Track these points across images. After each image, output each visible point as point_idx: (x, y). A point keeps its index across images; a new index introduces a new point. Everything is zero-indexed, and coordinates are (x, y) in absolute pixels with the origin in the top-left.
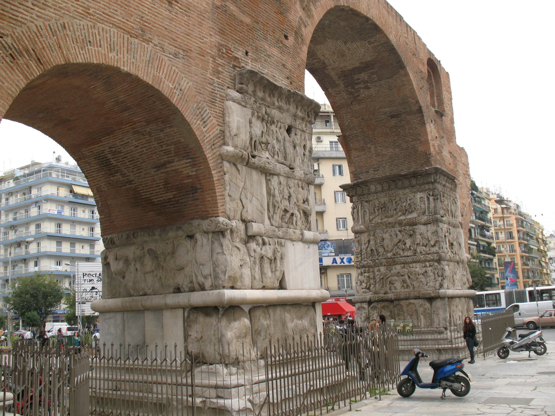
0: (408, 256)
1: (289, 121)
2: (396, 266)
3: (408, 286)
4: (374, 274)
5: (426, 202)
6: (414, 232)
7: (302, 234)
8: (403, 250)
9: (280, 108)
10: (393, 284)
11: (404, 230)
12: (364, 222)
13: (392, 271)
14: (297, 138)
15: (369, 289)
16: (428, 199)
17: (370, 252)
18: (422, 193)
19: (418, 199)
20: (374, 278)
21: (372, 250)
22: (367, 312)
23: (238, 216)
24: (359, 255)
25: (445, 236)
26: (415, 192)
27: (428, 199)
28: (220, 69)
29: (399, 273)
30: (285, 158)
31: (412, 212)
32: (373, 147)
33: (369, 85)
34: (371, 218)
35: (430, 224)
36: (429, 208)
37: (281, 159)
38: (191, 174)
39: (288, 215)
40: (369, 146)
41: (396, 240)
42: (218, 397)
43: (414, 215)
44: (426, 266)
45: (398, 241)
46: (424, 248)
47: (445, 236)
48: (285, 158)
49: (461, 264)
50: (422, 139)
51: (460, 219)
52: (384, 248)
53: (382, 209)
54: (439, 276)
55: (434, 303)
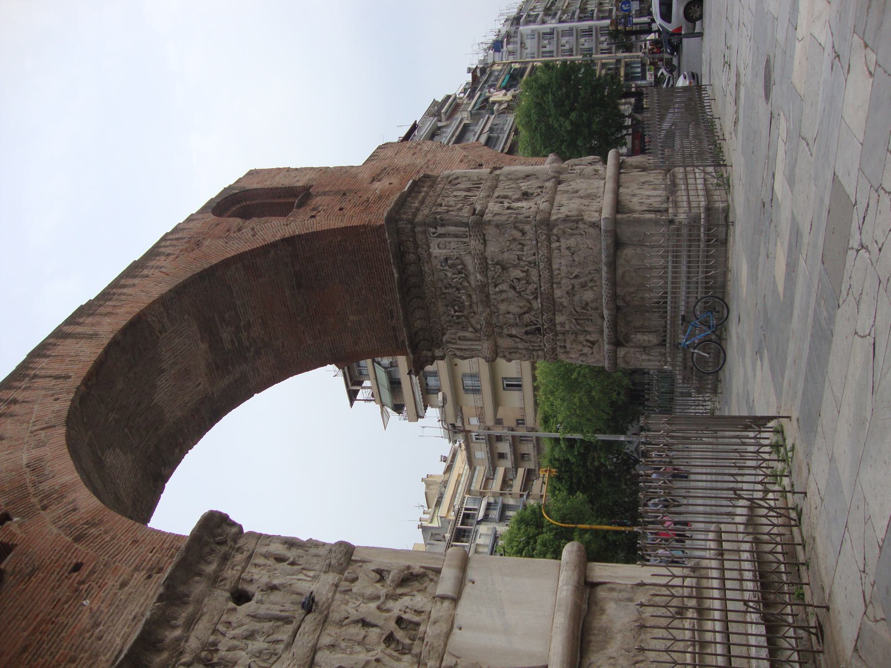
0: (540, 276)
1: (221, 597)
2: (556, 296)
3: (592, 280)
4: (568, 331)
6: (497, 263)
7: (443, 598)
8: (528, 283)
9: (190, 623)
10: (587, 304)
11: (493, 278)
13: (565, 304)
14: (260, 576)
15: (593, 343)
17: (529, 336)
18: (431, 245)
21: (527, 333)
22: (632, 350)
24: (535, 353)
25: (508, 208)
26: (430, 255)
29: (568, 293)
30: (287, 621)
31: (463, 263)
33: (242, 324)
34: (471, 329)
35: (484, 235)
36: (456, 236)
37: (284, 634)
39: (400, 635)
40: (349, 324)
41: (511, 294)
43: (469, 261)
44: (559, 248)
45: (511, 290)
46: (525, 248)
47: (508, 208)
48: (287, 621)
49: (562, 177)
51: (485, 170)
52: (525, 313)
53: (455, 311)
54: (577, 228)
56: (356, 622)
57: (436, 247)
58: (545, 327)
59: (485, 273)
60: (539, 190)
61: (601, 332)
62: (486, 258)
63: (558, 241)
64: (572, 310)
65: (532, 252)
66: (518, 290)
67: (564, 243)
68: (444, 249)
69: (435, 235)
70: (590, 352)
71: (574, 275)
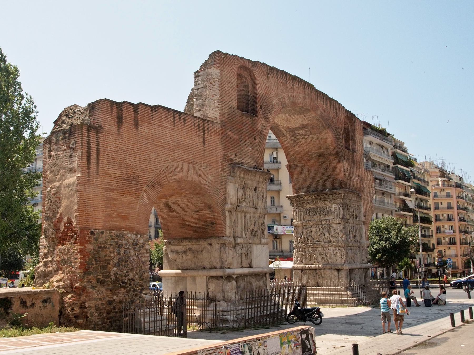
5: (338, 211)
8: (323, 239)
12: (300, 220)
15: (302, 261)
18: (336, 205)
19: (334, 208)
20: (305, 255)
22: (300, 275)
23: (232, 236)
24: (297, 240)
25: (350, 231)
28: (224, 167)
32: (307, 173)
33: (305, 137)
36: (339, 214)
38: (211, 216)
40: (304, 172)
42: (223, 315)
48: (253, 205)
49: (361, 248)
50: (338, 171)
51: (363, 219)
55: (340, 272)
56: (255, 221)
60: (356, 241)
63: (339, 250)
67: (338, 252)
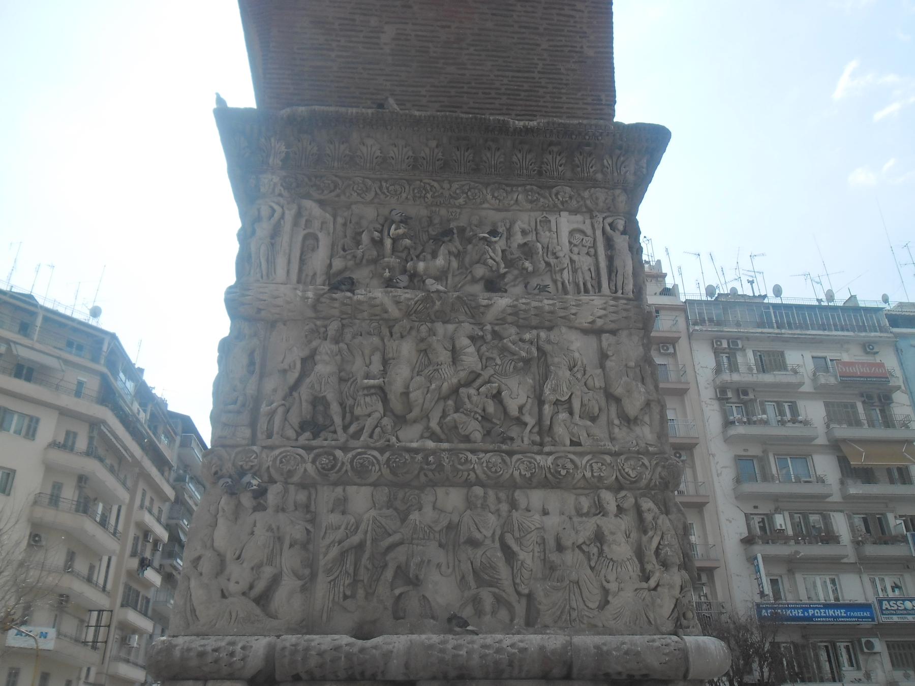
2: (440, 491)
13: (414, 516)
15: (263, 600)
16: (609, 244)
17: (306, 407)
18: (579, 218)
19: (564, 239)
21: (318, 402)
26: (556, 209)
27: (609, 244)
35: (613, 332)
41: (450, 377)
44: (600, 509)
52: (385, 400)
53: (395, 240)
54: (665, 565)
57: (575, 226)
58: (339, 453)
59: (510, 319)
61: (307, 626)
62: (550, 329)
63: (620, 510)
64: (396, 538)
65: (583, 438)
66: (463, 391)
68: (570, 243)
69: (608, 228)
70: (232, 587)
71: (515, 548)
